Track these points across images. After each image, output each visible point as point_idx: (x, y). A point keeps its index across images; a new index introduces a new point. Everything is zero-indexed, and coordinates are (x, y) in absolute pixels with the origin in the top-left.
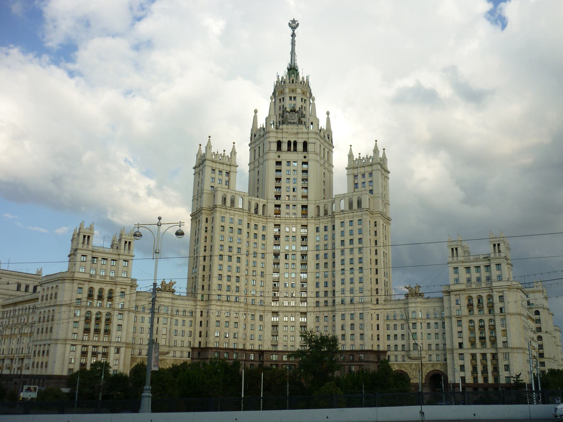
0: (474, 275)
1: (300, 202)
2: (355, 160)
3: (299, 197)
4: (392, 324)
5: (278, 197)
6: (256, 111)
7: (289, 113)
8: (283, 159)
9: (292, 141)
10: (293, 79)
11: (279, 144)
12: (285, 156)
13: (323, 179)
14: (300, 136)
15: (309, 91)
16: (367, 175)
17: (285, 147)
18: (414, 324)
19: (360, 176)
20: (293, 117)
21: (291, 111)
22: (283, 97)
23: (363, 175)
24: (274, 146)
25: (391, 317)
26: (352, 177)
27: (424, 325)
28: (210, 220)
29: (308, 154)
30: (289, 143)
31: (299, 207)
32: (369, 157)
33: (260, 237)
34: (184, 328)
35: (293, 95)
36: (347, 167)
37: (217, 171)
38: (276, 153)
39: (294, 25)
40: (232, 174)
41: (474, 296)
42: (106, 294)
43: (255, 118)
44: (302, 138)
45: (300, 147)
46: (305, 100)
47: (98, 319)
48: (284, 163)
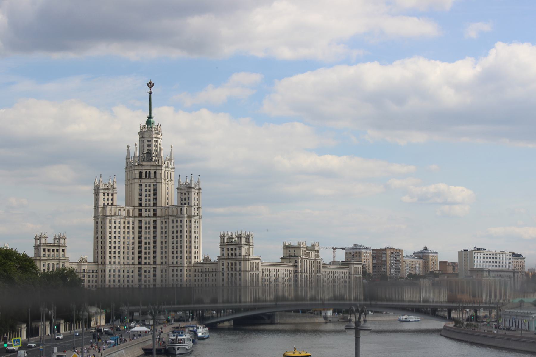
0: (230, 252)
3: (152, 205)
4: (197, 274)
5: (140, 205)
6: (128, 147)
7: (146, 154)
9: (148, 172)
11: (141, 173)
12: (145, 181)
16: (187, 194)
17: (144, 175)
18: (206, 274)
19: (183, 194)
20: (148, 156)
21: (147, 153)
23: (185, 194)
24: (137, 176)
25: (197, 271)
26: (180, 194)
27: (211, 275)
28: (103, 222)
29: (157, 179)
31: (152, 210)
33: (131, 228)
34: (92, 279)
35: (149, 139)
37: (106, 194)
39: (150, 85)
40: (114, 195)
41: (230, 262)
43: (128, 150)
44: (153, 170)
45: (152, 175)
48: (143, 185)
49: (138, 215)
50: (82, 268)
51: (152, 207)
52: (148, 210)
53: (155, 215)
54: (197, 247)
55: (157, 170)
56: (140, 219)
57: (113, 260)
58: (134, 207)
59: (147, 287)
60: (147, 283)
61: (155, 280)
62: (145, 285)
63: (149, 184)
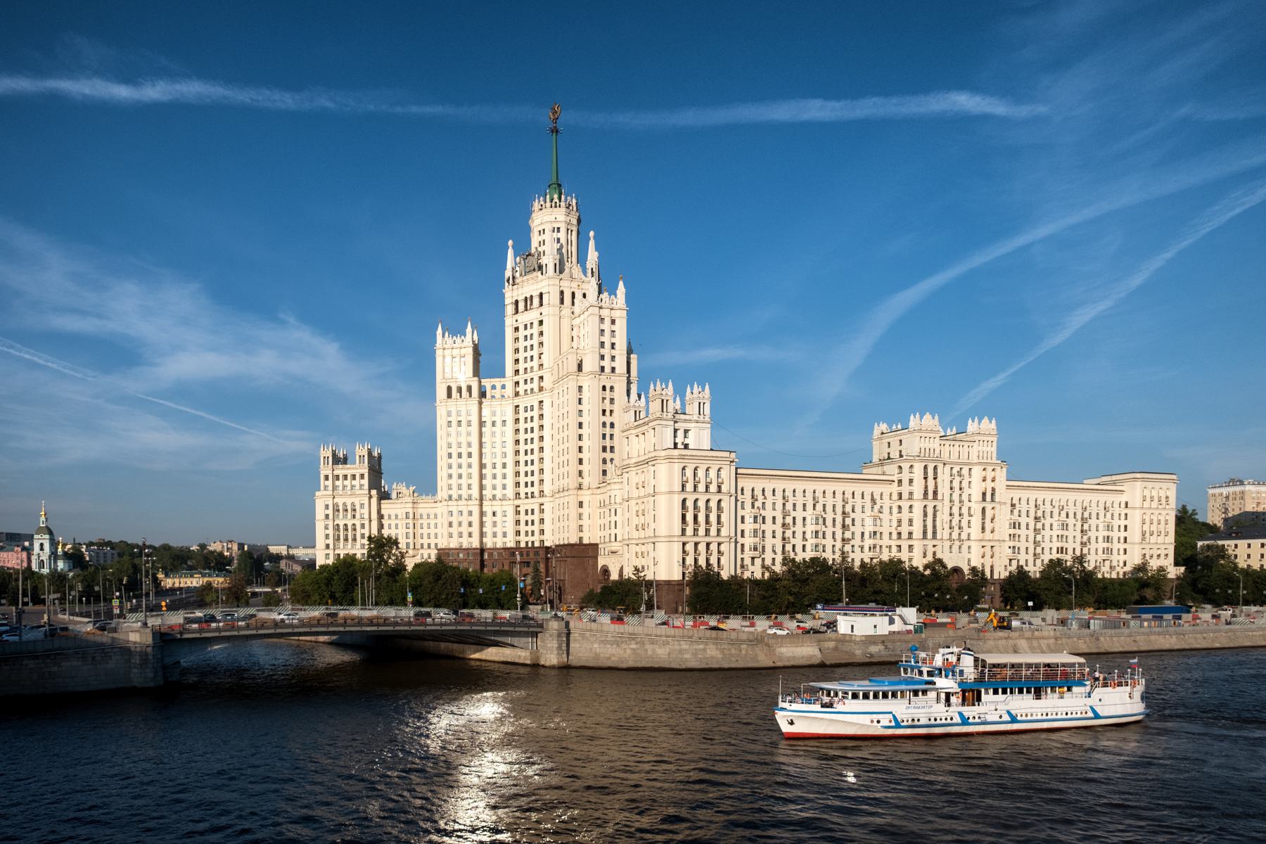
3: (536, 368)
9: (528, 297)
12: (524, 318)
17: (521, 306)
31: (536, 380)
34: (429, 531)
42: (349, 508)
47: (346, 530)
48: (521, 328)
50: (404, 511)
52: (529, 381)
53: (541, 389)
54: (612, 448)
56: (517, 401)
57: (455, 494)
59: (530, 545)
60: (530, 538)
61: (542, 532)
62: (527, 543)
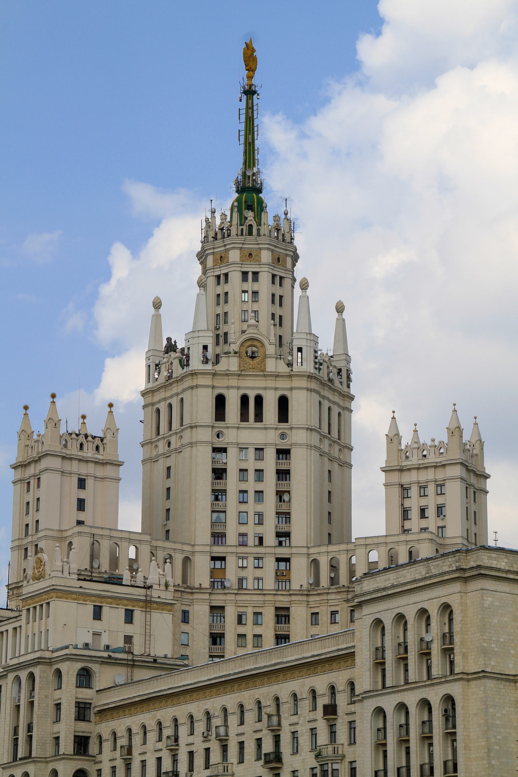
1: (272, 550)
2: (403, 447)
3: (270, 539)
8: (232, 443)
10: (251, 223)
13: (327, 487)
14: (271, 383)
15: (292, 254)
22: (225, 271)
26: (396, 491)
29: (291, 428)
30: (244, 399)
32: (437, 443)
35: (250, 269)
36: (384, 465)
38: (213, 427)
44: (276, 389)
46: (281, 278)
49: (206, 584)
51: (269, 550)
55: (291, 389)
58: (187, 548)
63: (256, 449)
